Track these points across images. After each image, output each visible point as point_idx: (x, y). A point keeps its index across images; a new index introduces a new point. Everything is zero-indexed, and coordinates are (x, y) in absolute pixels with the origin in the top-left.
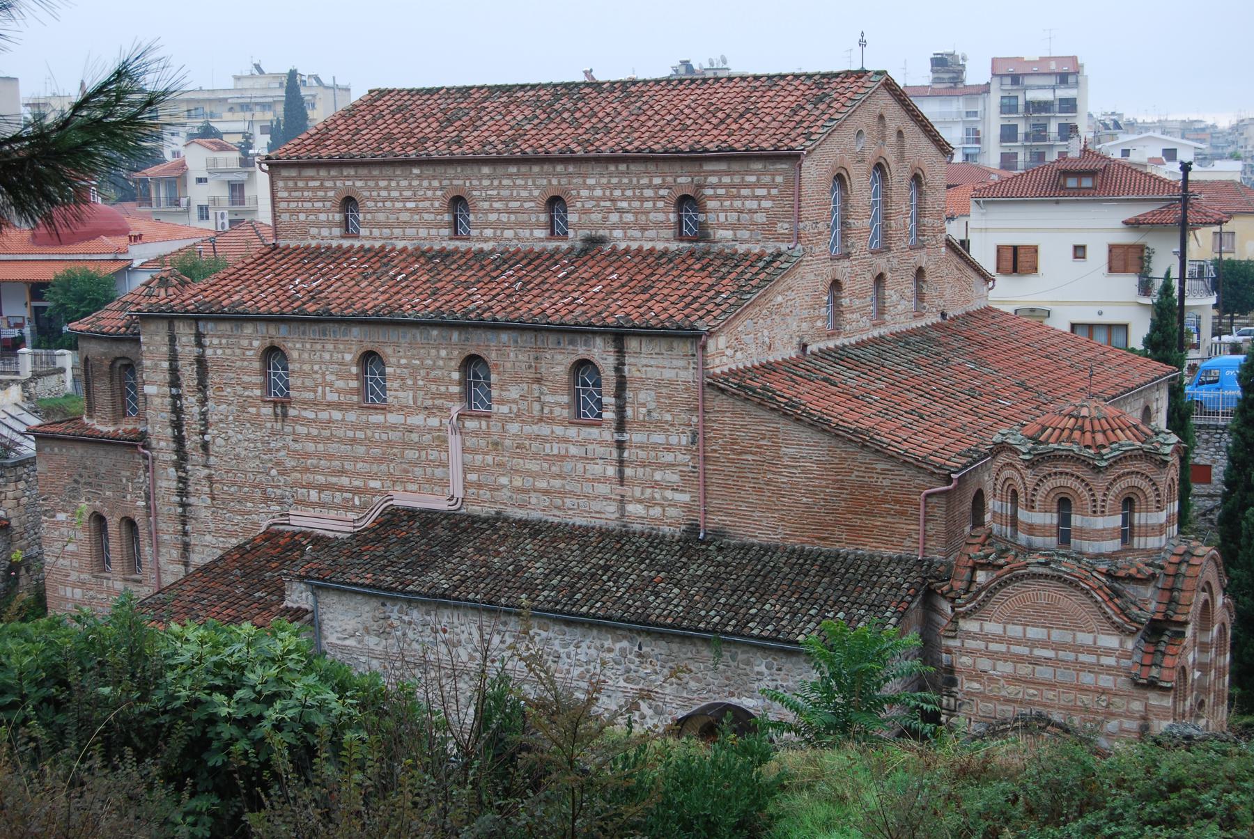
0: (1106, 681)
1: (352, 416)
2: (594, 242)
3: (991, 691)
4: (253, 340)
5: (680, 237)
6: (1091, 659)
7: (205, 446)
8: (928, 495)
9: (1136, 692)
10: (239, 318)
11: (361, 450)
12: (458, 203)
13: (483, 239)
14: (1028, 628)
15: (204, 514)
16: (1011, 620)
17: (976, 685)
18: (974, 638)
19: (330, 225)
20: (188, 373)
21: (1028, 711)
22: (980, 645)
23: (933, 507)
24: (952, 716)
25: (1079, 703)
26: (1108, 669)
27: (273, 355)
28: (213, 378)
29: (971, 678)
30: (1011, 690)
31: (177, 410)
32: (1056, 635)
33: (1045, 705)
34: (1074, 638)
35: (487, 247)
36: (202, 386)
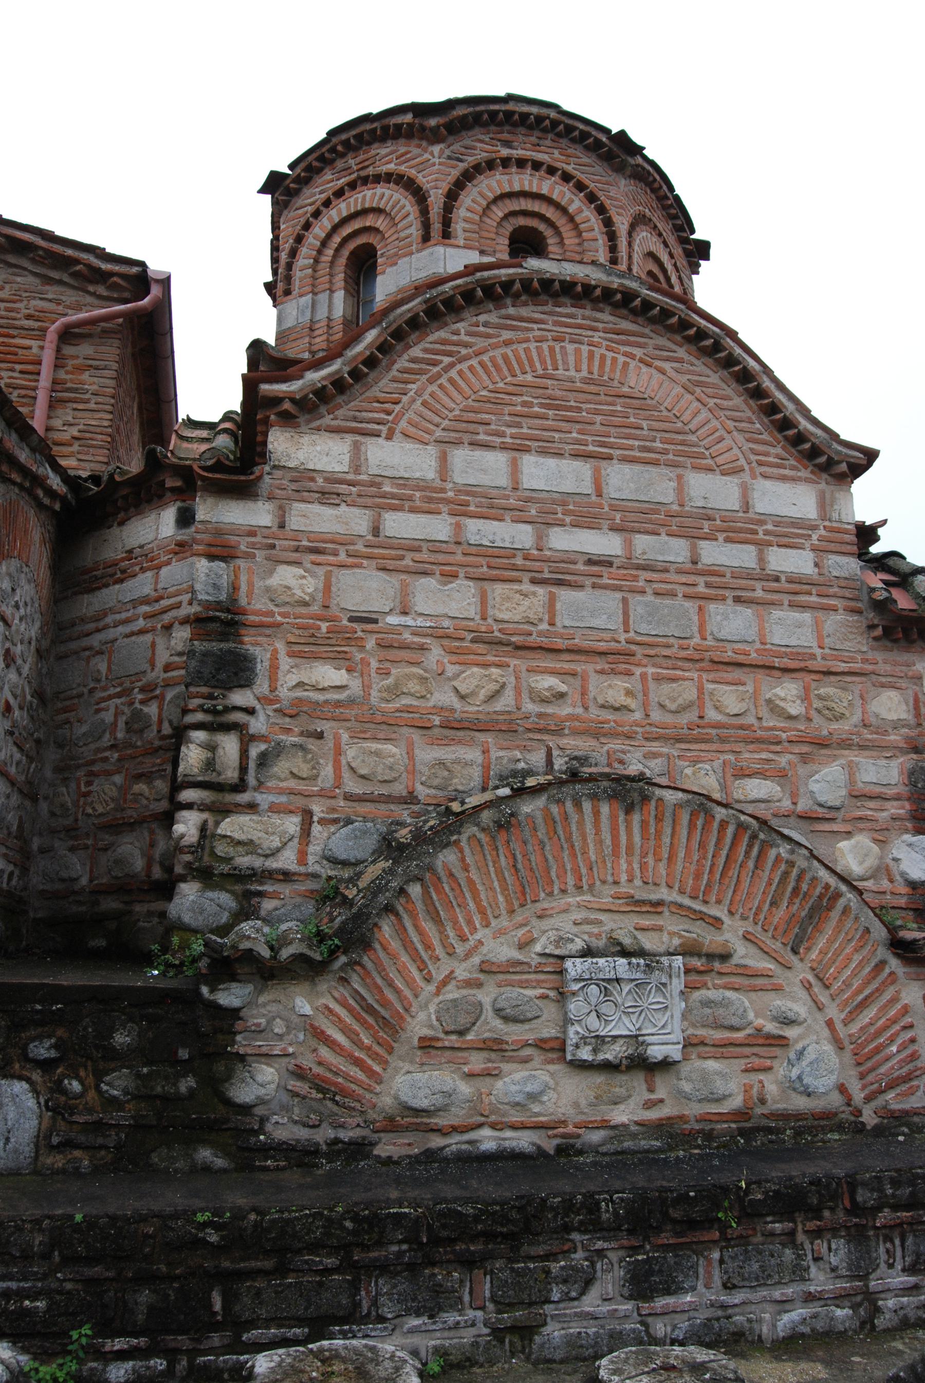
0: (791, 629)
3: (395, 691)
6: (742, 557)
8: (67, 335)
9: (884, 660)
14: (529, 462)
16: (467, 431)
17: (329, 675)
18: (326, 497)
21: (537, 759)
22: (352, 520)
23: (80, 369)
24: (223, 811)
25: (712, 715)
26: (794, 590)
29: (310, 648)
30: (473, 684)
32: (622, 481)
33: (597, 732)
34: (680, 490)
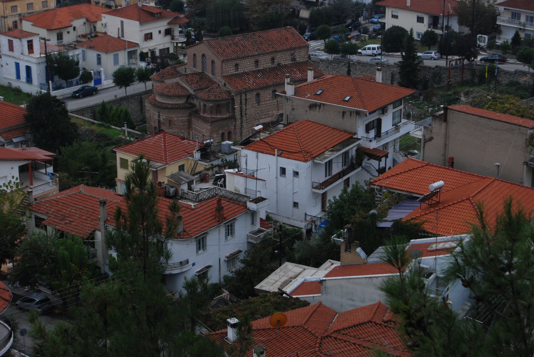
1: (271, 101)
2: (279, 64)
4: (255, 93)
5: (292, 61)
7: (246, 114)
10: (252, 90)
11: (272, 107)
12: (257, 62)
13: (261, 67)
15: (245, 126)
19: (233, 70)
20: (244, 101)
27: (258, 95)
28: (248, 101)
31: (241, 109)
35: (262, 68)
36: (246, 103)
